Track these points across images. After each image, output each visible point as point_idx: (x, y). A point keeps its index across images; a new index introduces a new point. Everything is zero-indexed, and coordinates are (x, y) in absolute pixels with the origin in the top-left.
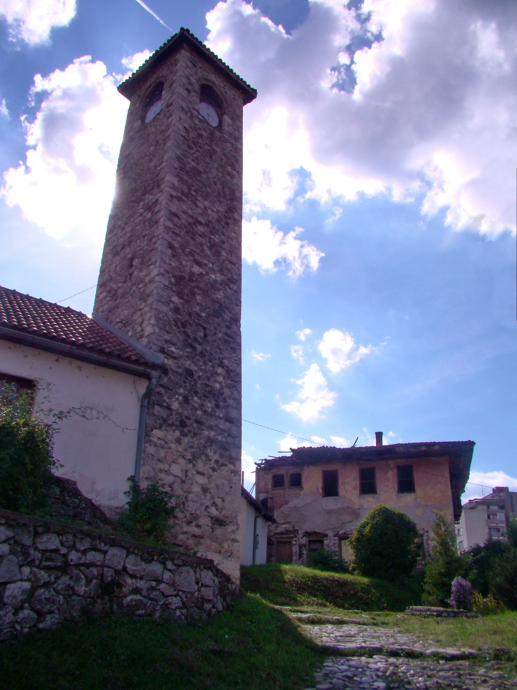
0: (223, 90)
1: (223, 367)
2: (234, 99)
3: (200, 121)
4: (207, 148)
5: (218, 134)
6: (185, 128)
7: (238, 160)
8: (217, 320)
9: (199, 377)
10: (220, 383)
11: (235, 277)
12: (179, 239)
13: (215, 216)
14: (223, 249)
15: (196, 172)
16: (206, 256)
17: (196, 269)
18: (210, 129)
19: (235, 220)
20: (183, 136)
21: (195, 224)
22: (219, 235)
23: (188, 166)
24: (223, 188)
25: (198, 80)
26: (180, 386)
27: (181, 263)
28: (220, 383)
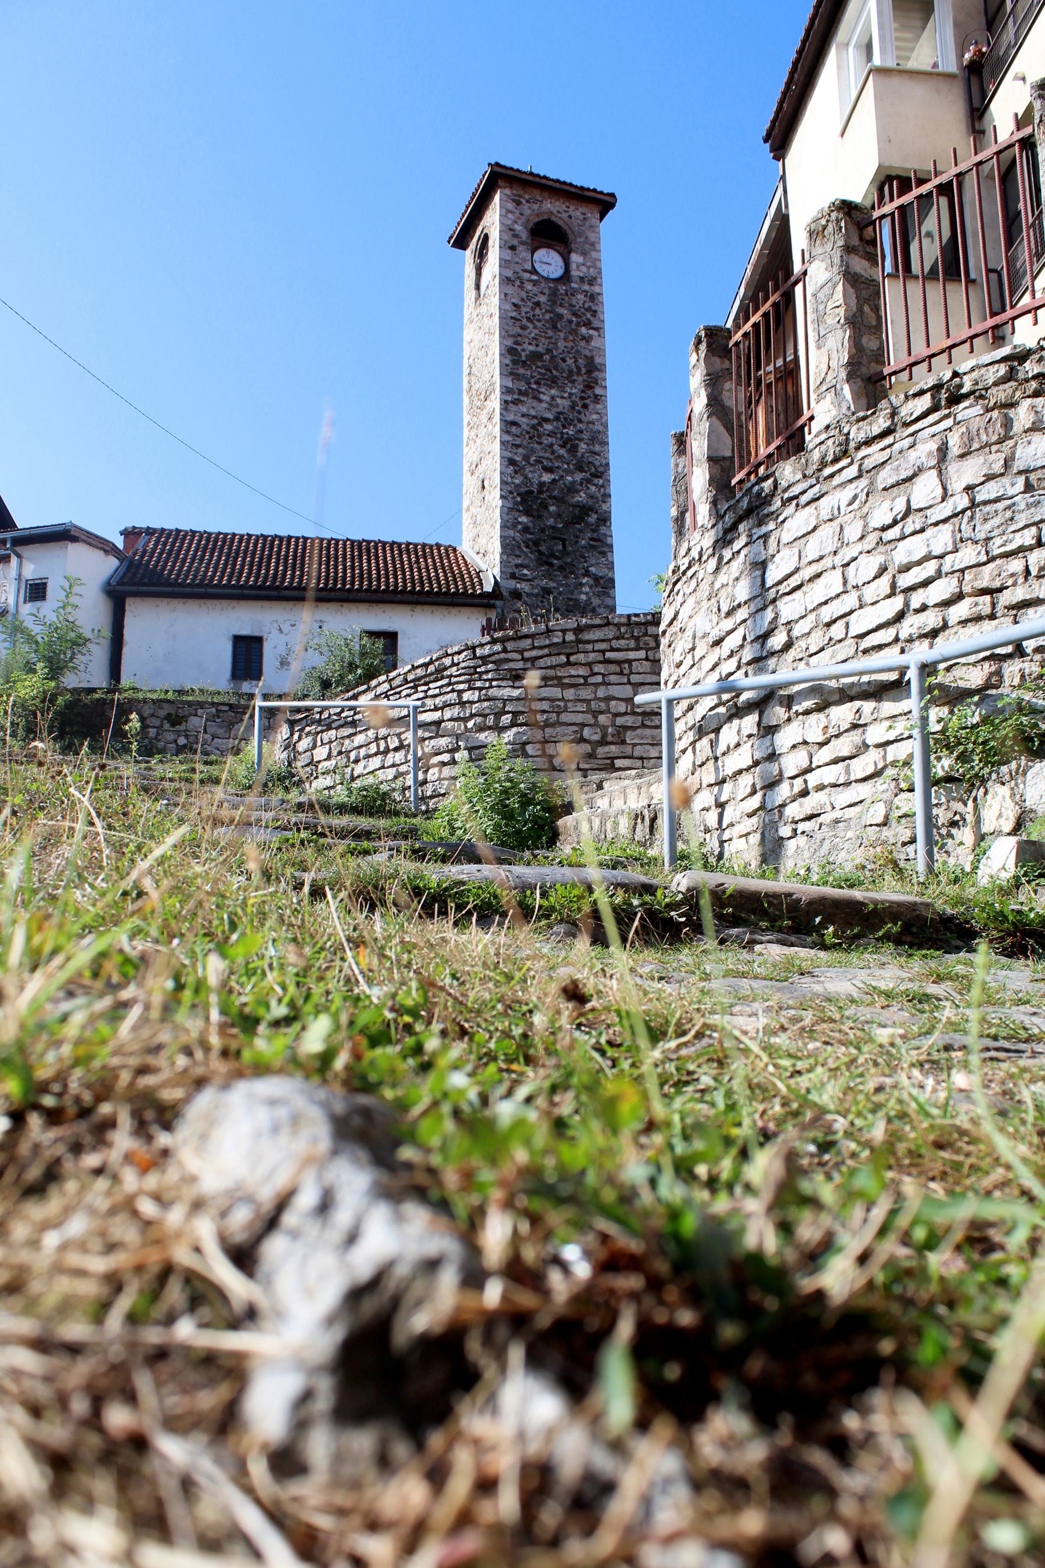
0: (565, 216)
3: (535, 283)
4: (547, 316)
5: (562, 289)
6: (514, 305)
11: (601, 469)
12: (521, 450)
13: (567, 403)
14: (580, 440)
15: (536, 356)
17: (547, 478)
21: (540, 424)
24: (576, 361)
27: (526, 477)
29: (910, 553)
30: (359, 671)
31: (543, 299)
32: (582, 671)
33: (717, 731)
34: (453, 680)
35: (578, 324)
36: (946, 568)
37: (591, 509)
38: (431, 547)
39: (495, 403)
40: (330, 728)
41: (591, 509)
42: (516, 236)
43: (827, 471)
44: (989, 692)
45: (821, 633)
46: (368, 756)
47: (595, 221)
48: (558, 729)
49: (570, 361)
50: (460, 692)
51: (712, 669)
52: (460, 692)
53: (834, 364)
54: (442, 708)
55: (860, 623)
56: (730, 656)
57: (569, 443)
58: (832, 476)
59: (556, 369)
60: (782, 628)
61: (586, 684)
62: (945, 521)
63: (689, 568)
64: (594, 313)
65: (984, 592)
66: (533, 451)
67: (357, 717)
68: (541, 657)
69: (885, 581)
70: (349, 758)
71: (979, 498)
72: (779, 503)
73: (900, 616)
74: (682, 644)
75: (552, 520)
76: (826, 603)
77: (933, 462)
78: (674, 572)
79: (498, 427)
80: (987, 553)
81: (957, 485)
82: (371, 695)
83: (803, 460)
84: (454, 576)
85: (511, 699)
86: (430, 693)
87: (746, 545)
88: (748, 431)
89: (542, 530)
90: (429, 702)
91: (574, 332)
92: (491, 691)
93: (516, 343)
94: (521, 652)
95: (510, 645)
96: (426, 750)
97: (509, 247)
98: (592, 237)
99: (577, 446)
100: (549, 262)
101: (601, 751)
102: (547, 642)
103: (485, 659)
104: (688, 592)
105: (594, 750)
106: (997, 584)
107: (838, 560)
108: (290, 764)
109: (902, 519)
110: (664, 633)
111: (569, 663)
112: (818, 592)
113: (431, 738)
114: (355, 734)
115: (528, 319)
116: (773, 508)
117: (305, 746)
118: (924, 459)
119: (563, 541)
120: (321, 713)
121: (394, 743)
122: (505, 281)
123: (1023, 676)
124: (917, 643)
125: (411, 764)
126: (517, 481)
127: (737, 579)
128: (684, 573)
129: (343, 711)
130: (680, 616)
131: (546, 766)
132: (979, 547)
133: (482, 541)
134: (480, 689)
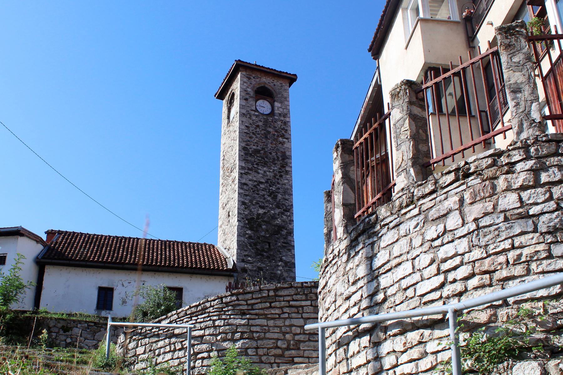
0: (272, 84)
1: (282, 261)
2: (282, 86)
3: (257, 116)
4: (263, 132)
5: (270, 119)
6: (246, 126)
7: (287, 130)
8: (277, 236)
9: (267, 270)
10: (281, 270)
11: (289, 207)
12: (248, 197)
13: (272, 174)
14: (278, 193)
15: (257, 151)
16: (268, 201)
17: (261, 211)
18: (264, 118)
19: (286, 171)
20: (245, 133)
21: (258, 185)
22: (276, 186)
23: (250, 150)
24: (277, 154)
25: (252, 89)
26: (256, 276)
27: (251, 211)
28: (281, 270)
29: (446, 253)
30: (163, 308)
31: (260, 124)
32: (277, 311)
33: (348, 344)
34: (211, 314)
35: (278, 136)
36: (466, 260)
37: (284, 227)
38: (201, 245)
39: (236, 174)
40: (145, 337)
41: (283, 227)
42: (248, 94)
43: (403, 211)
44: (491, 325)
45: (401, 294)
46: (165, 353)
47: (286, 87)
48: (265, 341)
49: (274, 154)
50: (214, 321)
51: (345, 312)
52: (214, 321)
53: (405, 158)
54: (204, 329)
55: (422, 288)
56: (355, 305)
57: (273, 195)
58: (405, 213)
59: (267, 157)
60: (381, 291)
61: (279, 318)
62: (464, 236)
63: (333, 259)
64: (286, 131)
65: (485, 272)
66: (254, 198)
67: (160, 332)
68: (257, 304)
69: (434, 267)
70: (155, 353)
71: (481, 225)
72: (379, 227)
73: (442, 285)
74: (329, 299)
75: (263, 233)
76: (404, 278)
77: (457, 206)
78: (325, 261)
79: (237, 186)
80: (486, 252)
81: (470, 218)
82: (168, 321)
83: (391, 206)
84: (213, 260)
85: (240, 325)
86: (198, 321)
87: (362, 248)
88: (363, 191)
89: (259, 238)
90: (198, 325)
91: (276, 140)
92: (230, 320)
93: (247, 145)
94: (246, 301)
95: (240, 297)
96: (195, 351)
97: (244, 99)
98: (285, 94)
99: (277, 195)
100: (264, 106)
101: (287, 353)
102: (260, 296)
103: (227, 304)
104: (332, 272)
105: (283, 353)
106: (492, 268)
107: (410, 256)
108: (124, 356)
109: (442, 235)
110: (320, 292)
111: (271, 307)
112: (400, 272)
113: (198, 344)
114: (158, 341)
115: (253, 133)
116: (376, 230)
117: (133, 346)
118: (452, 205)
119: (269, 243)
120: (141, 329)
121: (179, 346)
122: (242, 115)
123: (508, 316)
124: (452, 299)
125: (187, 357)
126: (246, 213)
127: (358, 266)
128: (331, 262)
129: (153, 329)
130: (328, 284)
131: (258, 361)
132: (482, 250)
133: (228, 242)
134: (225, 319)
